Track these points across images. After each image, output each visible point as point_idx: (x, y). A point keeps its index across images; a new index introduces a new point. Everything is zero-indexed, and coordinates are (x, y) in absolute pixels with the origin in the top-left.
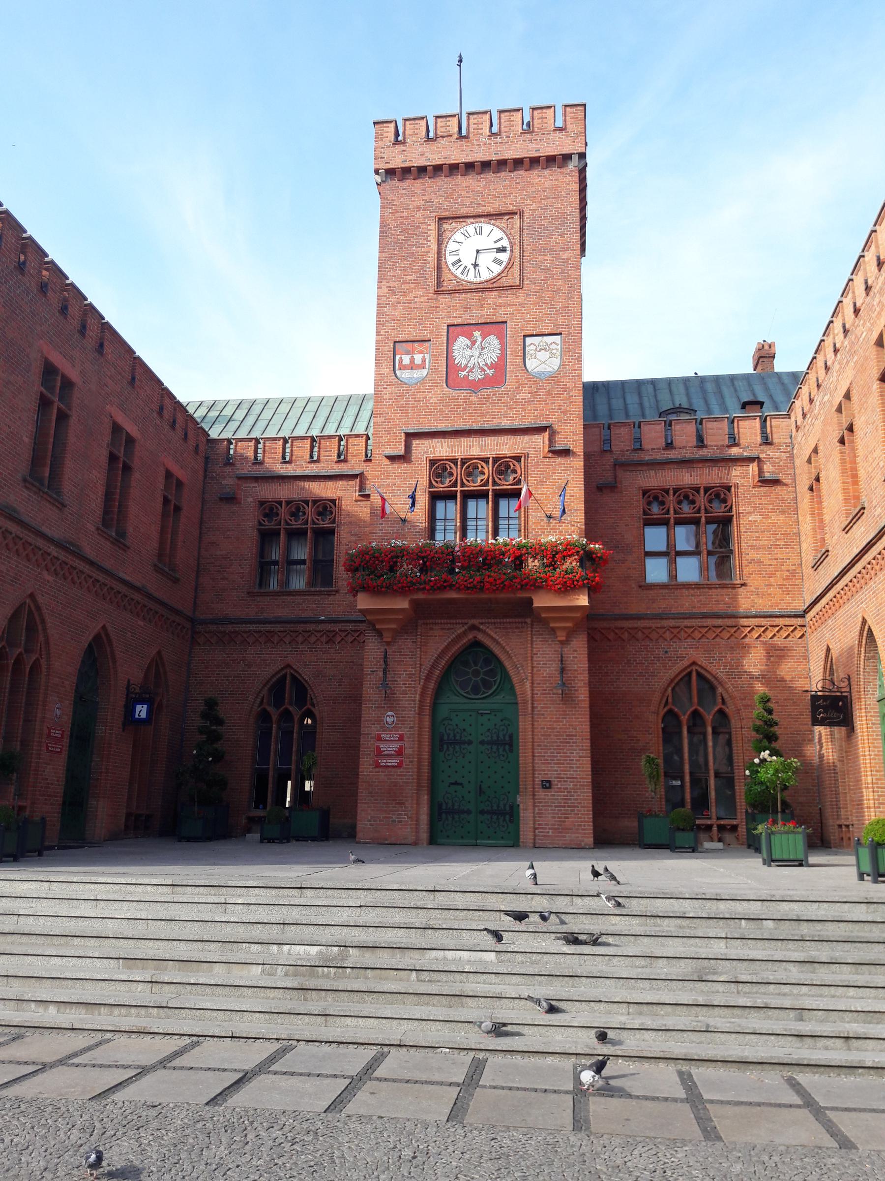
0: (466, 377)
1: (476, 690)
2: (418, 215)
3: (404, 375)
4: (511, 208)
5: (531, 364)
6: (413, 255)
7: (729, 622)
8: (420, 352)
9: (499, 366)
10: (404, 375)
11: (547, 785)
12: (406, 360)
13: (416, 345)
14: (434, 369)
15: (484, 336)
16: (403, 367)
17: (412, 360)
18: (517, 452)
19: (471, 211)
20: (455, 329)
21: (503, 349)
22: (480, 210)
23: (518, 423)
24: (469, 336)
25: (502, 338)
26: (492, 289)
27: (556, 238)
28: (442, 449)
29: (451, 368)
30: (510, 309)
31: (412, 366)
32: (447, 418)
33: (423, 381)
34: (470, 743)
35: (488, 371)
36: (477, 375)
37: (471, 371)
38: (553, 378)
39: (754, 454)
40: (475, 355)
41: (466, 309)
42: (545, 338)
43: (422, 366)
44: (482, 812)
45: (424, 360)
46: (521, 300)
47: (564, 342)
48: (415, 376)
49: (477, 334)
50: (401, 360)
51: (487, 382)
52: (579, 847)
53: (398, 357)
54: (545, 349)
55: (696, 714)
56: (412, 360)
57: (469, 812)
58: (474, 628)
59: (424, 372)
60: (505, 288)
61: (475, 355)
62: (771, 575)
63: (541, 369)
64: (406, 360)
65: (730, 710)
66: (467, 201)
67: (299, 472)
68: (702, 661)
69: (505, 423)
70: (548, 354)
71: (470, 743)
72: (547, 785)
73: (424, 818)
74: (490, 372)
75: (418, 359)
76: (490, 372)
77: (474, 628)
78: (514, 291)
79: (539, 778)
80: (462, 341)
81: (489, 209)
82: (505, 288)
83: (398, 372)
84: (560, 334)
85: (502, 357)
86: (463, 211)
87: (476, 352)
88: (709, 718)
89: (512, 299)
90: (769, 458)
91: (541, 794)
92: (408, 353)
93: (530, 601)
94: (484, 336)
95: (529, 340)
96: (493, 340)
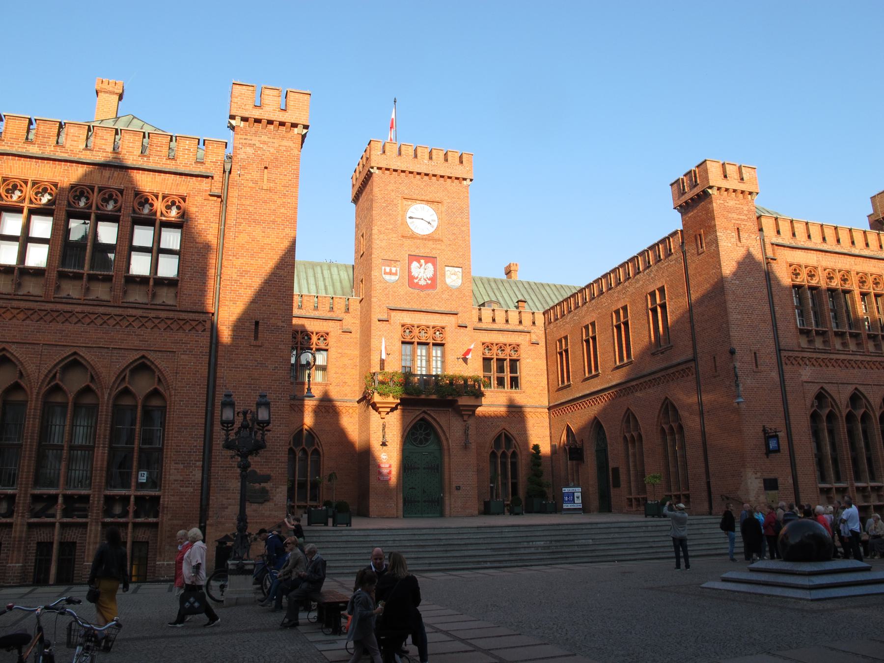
0: (417, 283)
1: (421, 443)
2: (393, 194)
3: (387, 277)
4: (438, 200)
6: (390, 215)
7: (518, 410)
9: (433, 279)
11: (458, 488)
14: (401, 277)
15: (426, 263)
16: (386, 273)
18: (443, 324)
19: (419, 197)
20: (413, 258)
21: (435, 271)
22: (423, 198)
23: (442, 310)
24: (419, 262)
25: (434, 265)
26: (429, 240)
27: (459, 219)
28: (407, 318)
29: (411, 278)
30: (438, 252)
31: (390, 273)
32: (409, 303)
34: (418, 468)
36: (422, 283)
38: (459, 289)
39: (529, 330)
40: (422, 272)
41: (417, 247)
44: (425, 501)
46: (443, 247)
49: (422, 261)
51: (427, 287)
52: (472, 516)
55: (504, 453)
57: (419, 502)
58: (424, 412)
59: (397, 277)
60: (436, 240)
61: (422, 272)
62: (535, 388)
65: (518, 451)
66: (417, 192)
67: (308, 315)
68: (507, 428)
69: (437, 309)
71: (418, 468)
72: (458, 488)
73: (401, 505)
74: (429, 282)
76: (429, 282)
77: (424, 412)
79: (454, 485)
80: (415, 264)
81: (427, 198)
82: (436, 240)
85: (435, 275)
86: (415, 197)
87: (422, 270)
88: (499, 455)
89: (438, 246)
90: (535, 333)
91: (456, 492)
93: (457, 401)
94: (426, 263)
95: (447, 268)
96: (430, 265)
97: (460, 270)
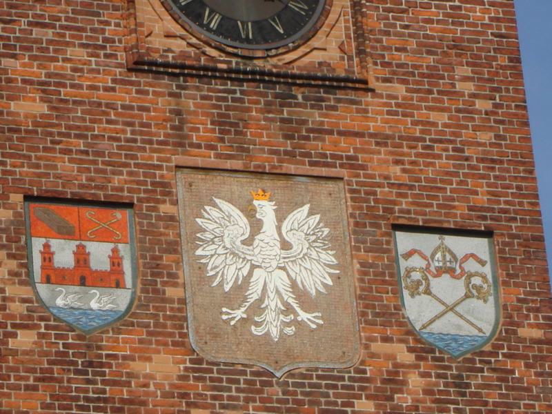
3: (63, 299)
5: (418, 310)
8: (103, 236)
10: (63, 299)
12: (64, 254)
13: (89, 212)
16: (54, 276)
17: (82, 257)
31: (83, 275)
33: (123, 322)
35: (303, 316)
37: (258, 308)
42: (451, 241)
43: (112, 278)
45: (116, 261)
47: (502, 259)
48: (94, 305)
50: (48, 256)
53: (37, 244)
54: (451, 271)
56: (82, 257)
59: (120, 299)
63: (448, 325)
64: (64, 254)
70: (459, 288)
75: (99, 254)
78: (352, 96)
83: (43, 290)
84: (488, 234)
89: (346, 118)
92: (66, 233)
95: (404, 241)
97: (480, 246)
